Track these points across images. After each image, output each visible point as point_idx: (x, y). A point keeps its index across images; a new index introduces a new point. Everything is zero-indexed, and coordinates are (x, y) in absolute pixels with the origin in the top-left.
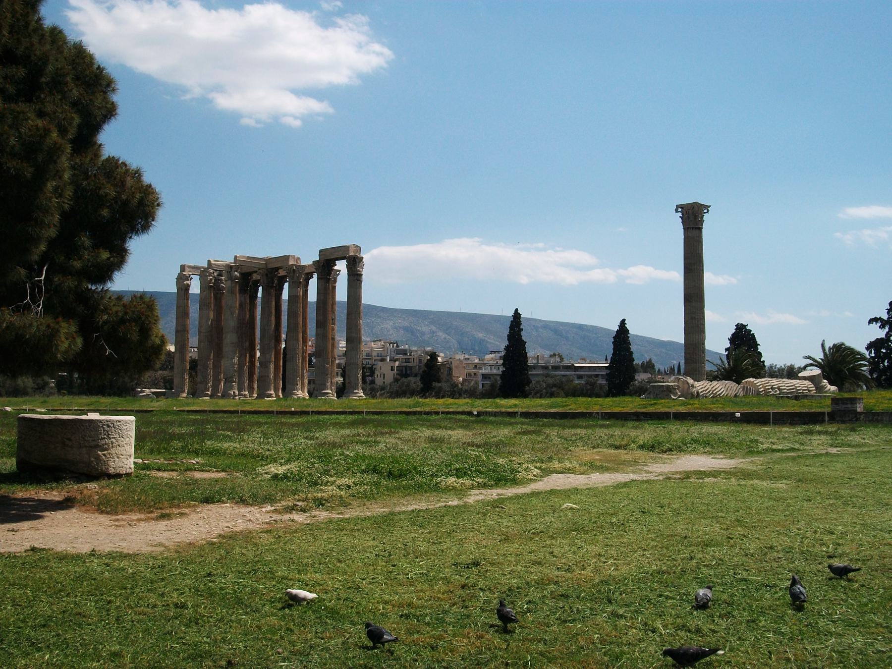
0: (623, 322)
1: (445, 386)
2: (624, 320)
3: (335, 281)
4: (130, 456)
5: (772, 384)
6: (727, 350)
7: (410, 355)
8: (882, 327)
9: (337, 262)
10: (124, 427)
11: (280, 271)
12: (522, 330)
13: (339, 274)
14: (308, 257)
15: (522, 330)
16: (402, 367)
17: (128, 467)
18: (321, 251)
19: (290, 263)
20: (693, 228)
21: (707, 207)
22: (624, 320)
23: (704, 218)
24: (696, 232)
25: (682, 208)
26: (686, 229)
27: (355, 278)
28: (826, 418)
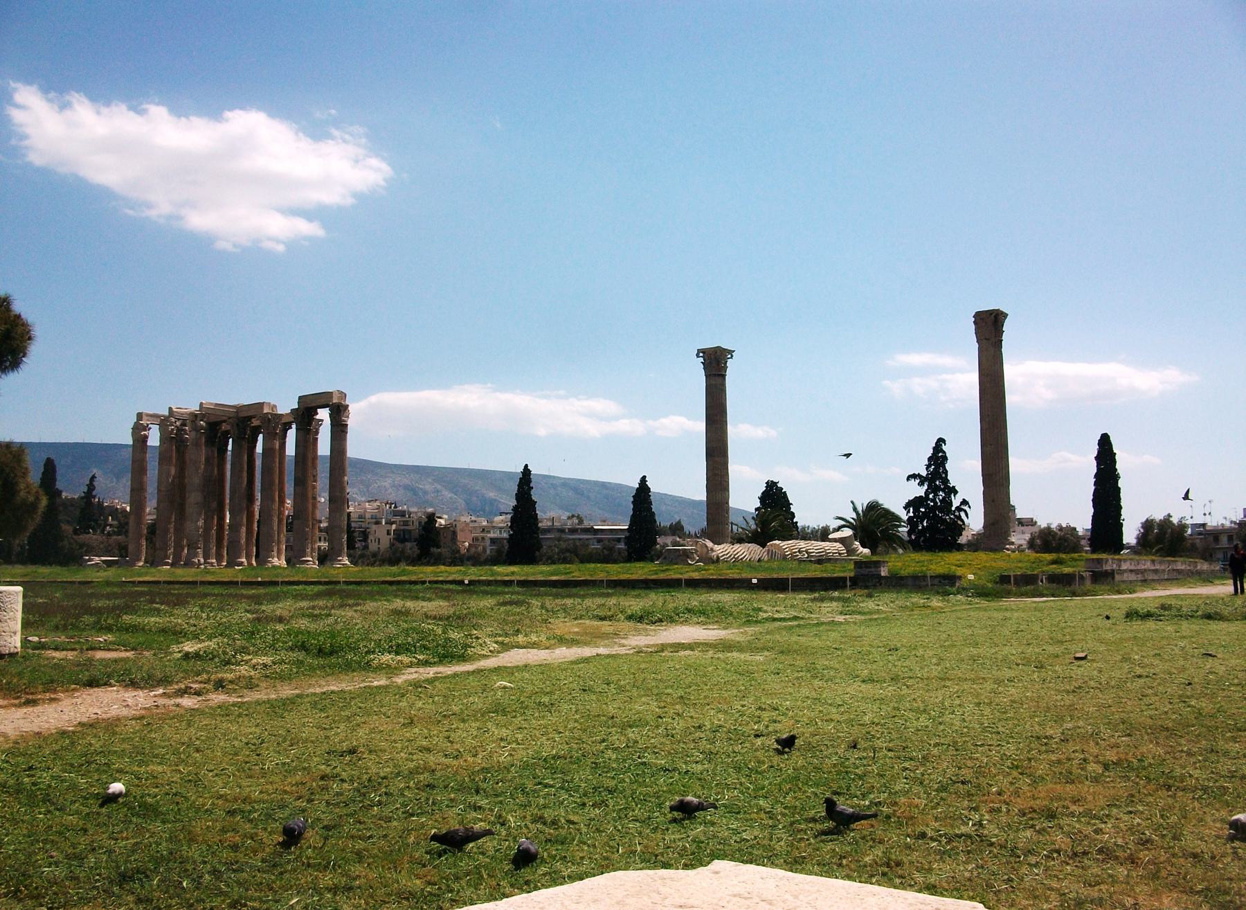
0: (644, 479)
1: (443, 551)
2: (644, 477)
3: (317, 433)
6: (756, 509)
7: (409, 517)
8: (921, 484)
9: (319, 410)
11: (253, 420)
14: (286, 405)
16: (401, 530)
18: (300, 398)
19: (265, 411)
22: (644, 477)
24: (719, 380)
25: (703, 353)
28: (848, 583)
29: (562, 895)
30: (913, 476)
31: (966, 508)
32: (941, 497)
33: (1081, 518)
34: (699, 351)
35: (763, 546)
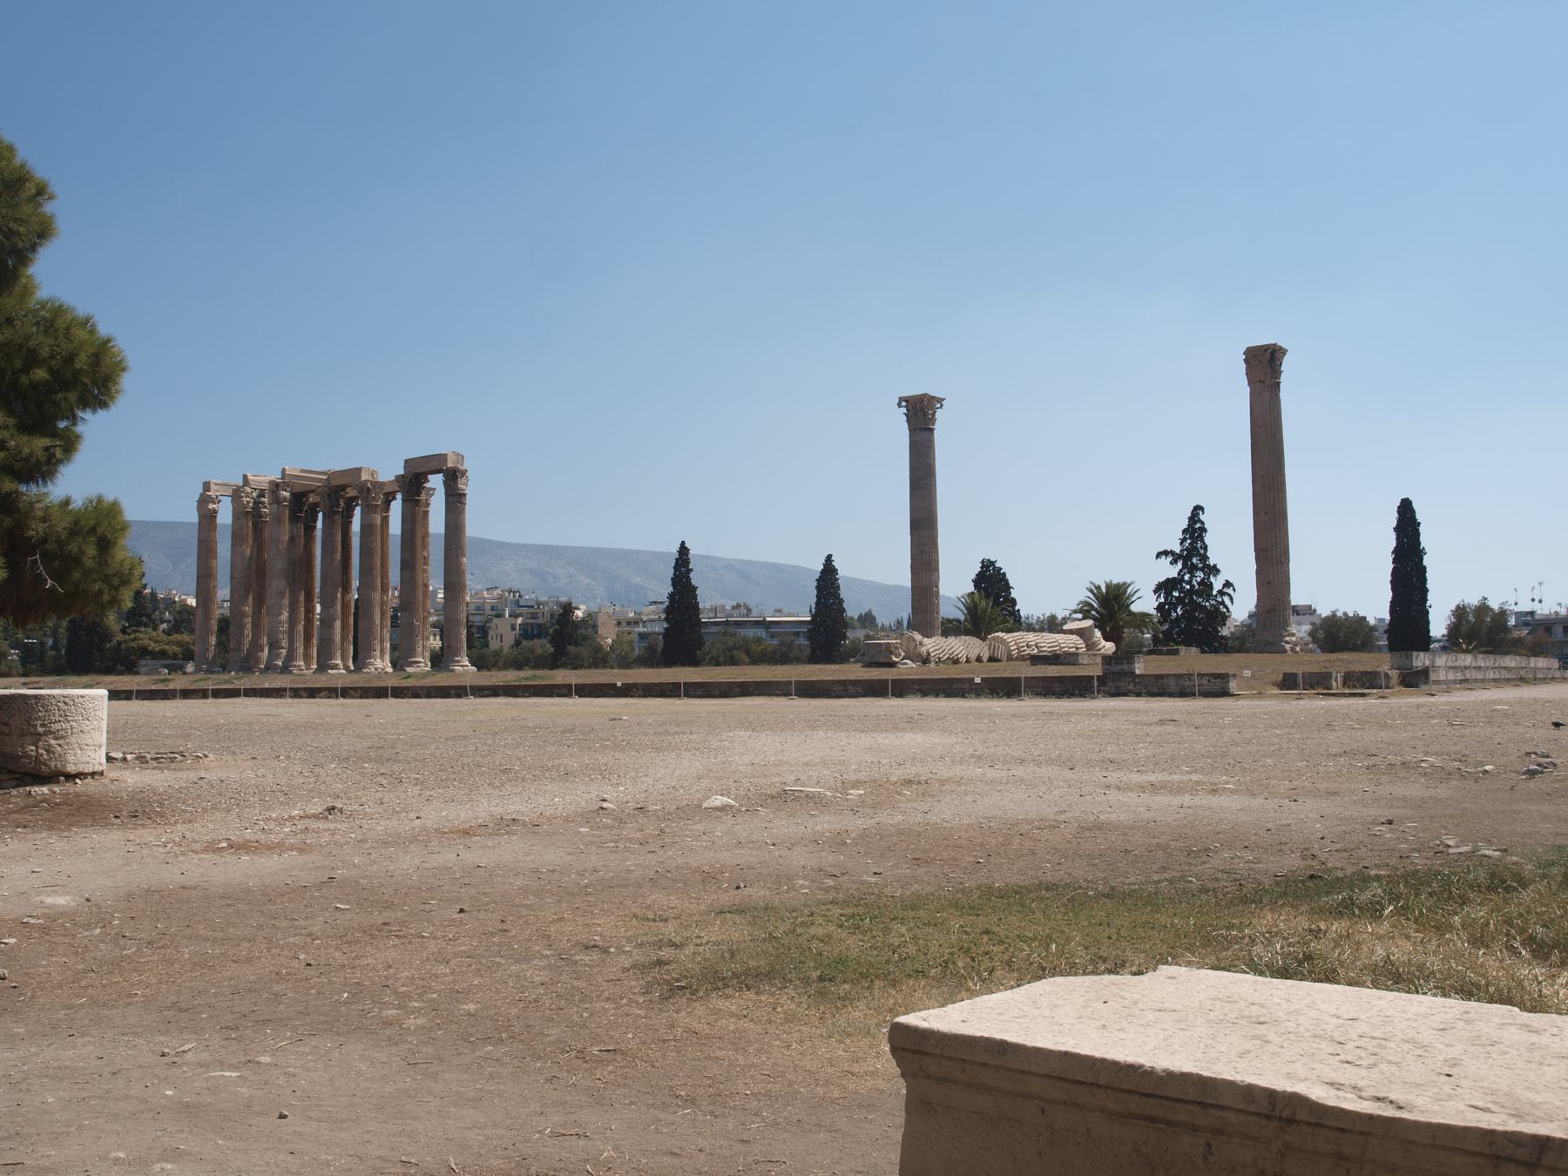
0: (829, 558)
1: (584, 651)
3: (428, 505)
4: (100, 746)
5: (1028, 640)
7: (538, 608)
8: (1174, 562)
10: (90, 706)
11: (348, 490)
12: (692, 570)
13: (432, 494)
14: (388, 470)
15: (692, 570)
16: (527, 624)
17: (96, 762)
18: (407, 462)
19: (363, 478)
20: (921, 429)
21: (940, 400)
23: (936, 416)
25: (907, 401)
27: (455, 499)
30: (1166, 553)
31: (1230, 591)
32: (1199, 579)
33: (1375, 605)
34: (901, 399)
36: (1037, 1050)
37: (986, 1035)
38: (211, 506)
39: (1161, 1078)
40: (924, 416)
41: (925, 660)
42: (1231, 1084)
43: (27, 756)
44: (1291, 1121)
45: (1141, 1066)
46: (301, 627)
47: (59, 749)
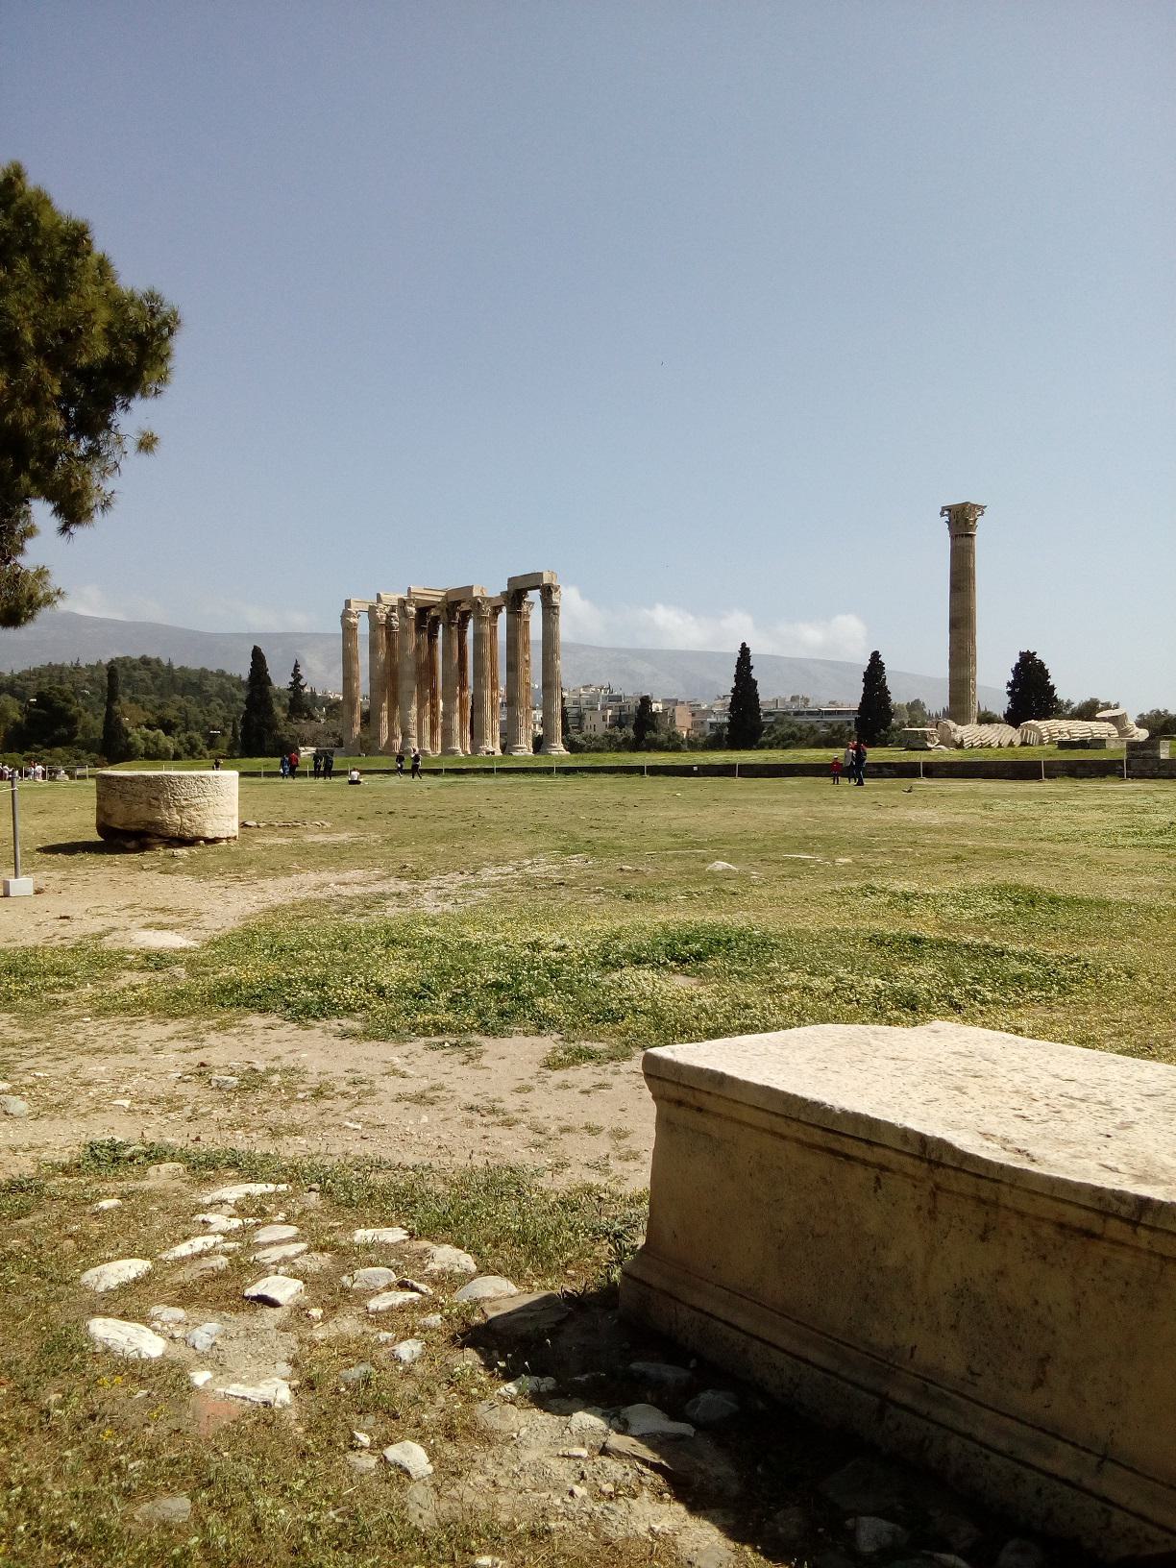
0: (875, 656)
4: (232, 816)
6: (1009, 685)
21: (981, 508)
25: (949, 510)
26: (954, 537)
27: (550, 609)
29: (765, 1041)
34: (944, 508)
35: (1016, 726)
36: (746, 1084)
37: (711, 1068)
38: (352, 620)
39: (837, 1116)
40: (966, 524)
41: (960, 746)
42: (890, 1126)
43: (175, 825)
44: (939, 1164)
45: (823, 1104)
46: (427, 719)
47: (199, 818)
